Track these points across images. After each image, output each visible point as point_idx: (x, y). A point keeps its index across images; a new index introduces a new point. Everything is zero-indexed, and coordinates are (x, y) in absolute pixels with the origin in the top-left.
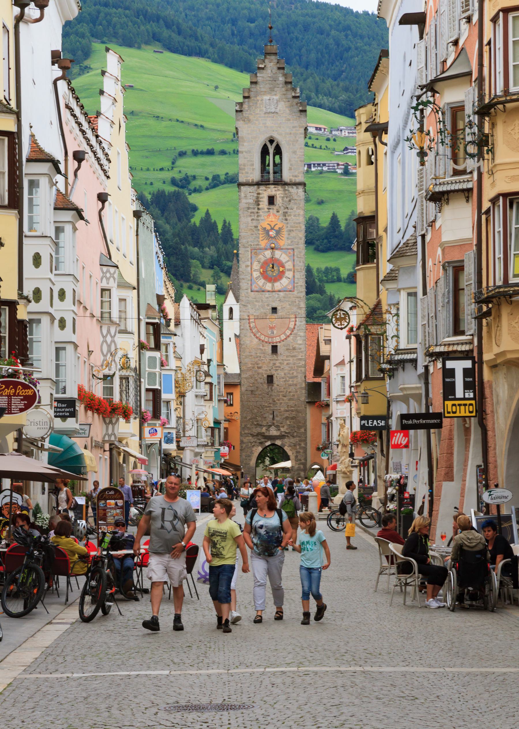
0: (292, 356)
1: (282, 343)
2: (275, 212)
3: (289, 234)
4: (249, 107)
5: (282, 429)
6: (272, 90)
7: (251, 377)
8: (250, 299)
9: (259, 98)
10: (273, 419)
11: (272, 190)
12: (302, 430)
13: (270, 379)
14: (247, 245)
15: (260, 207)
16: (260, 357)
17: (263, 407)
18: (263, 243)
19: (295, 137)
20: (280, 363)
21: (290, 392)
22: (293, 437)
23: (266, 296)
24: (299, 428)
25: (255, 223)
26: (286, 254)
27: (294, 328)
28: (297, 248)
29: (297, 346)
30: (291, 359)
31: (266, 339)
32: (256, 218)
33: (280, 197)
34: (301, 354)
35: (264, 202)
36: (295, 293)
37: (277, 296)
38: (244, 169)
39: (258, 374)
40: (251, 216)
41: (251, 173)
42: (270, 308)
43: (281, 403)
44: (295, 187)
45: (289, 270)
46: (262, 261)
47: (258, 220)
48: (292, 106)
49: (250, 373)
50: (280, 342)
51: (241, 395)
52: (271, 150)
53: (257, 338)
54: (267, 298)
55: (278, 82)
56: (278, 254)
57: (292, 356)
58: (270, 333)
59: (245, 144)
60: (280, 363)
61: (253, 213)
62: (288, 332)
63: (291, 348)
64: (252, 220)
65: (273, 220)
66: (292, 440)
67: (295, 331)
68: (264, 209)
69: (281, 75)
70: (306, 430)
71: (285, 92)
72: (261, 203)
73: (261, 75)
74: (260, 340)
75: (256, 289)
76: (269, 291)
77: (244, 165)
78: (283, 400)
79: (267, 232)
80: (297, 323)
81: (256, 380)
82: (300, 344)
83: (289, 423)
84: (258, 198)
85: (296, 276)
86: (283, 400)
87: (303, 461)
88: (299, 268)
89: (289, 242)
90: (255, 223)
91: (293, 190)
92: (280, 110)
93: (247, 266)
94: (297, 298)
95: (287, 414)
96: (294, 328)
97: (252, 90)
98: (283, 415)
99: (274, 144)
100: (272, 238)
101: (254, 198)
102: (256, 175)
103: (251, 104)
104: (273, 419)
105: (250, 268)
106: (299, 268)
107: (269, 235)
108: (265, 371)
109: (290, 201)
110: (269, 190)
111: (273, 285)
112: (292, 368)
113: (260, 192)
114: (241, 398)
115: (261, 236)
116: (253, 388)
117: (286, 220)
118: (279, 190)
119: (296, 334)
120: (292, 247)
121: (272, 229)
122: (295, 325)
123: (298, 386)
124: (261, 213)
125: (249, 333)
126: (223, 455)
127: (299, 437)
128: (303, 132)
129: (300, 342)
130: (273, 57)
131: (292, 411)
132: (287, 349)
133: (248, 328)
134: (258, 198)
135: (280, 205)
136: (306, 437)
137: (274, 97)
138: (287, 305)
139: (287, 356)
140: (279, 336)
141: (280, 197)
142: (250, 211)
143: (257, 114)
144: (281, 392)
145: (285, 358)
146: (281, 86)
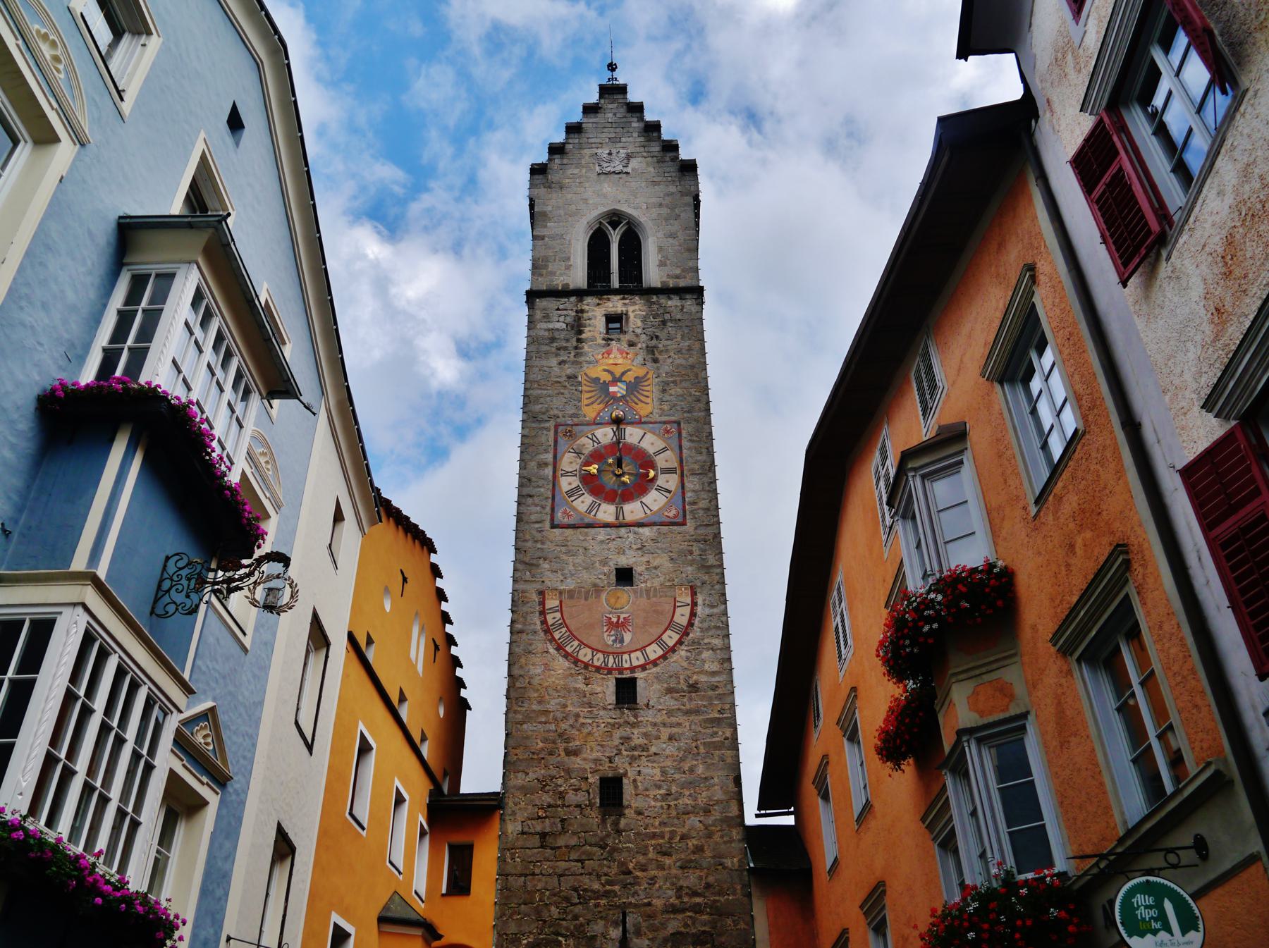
0: (688, 713)
2: (624, 346)
3: (664, 391)
6: (614, 141)
7: (543, 784)
9: (587, 152)
11: (616, 304)
13: (611, 789)
14: (545, 417)
15: (583, 336)
16: (577, 716)
17: (584, 896)
20: (645, 735)
21: (683, 837)
23: (600, 537)
27: (690, 624)
28: (688, 421)
29: (703, 678)
31: (598, 660)
37: (631, 536)
39: (568, 772)
40: (557, 355)
46: (586, 452)
49: (537, 772)
50: (643, 667)
51: (502, 850)
52: (615, 237)
53: (567, 655)
54: (602, 542)
56: (632, 435)
57: (688, 713)
58: (610, 640)
60: (645, 735)
61: (565, 348)
62: (671, 638)
65: (620, 361)
67: (695, 634)
68: (593, 339)
72: (586, 329)
74: (576, 661)
75: (566, 521)
76: (607, 525)
78: (661, 867)
80: (699, 609)
81: (562, 795)
82: (714, 674)
86: (661, 867)
88: (696, 467)
93: (542, 465)
95: (674, 925)
96: (690, 624)
98: (664, 925)
99: (621, 230)
103: (565, 161)
107: (607, 393)
108: (591, 759)
109: (664, 323)
111: (620, 511)
113: (586, 307)
114: (502, 860)
116: (547, 826)
117: (655, 361)
118: (635, 304)
119: (696, 643)
120: (673, 418)
121: (615, 381)
122: (693, 614)
123: (716, 814)
124: (586, 348)
125: (540, 642)
131: (697, 909)
132: (670, 691)
133: (538, 627)
135: (639, 331)
138: (662, 560)
139: (670, 713)
140: (642, 649)
144: (654, 836)
146: (635, 135)
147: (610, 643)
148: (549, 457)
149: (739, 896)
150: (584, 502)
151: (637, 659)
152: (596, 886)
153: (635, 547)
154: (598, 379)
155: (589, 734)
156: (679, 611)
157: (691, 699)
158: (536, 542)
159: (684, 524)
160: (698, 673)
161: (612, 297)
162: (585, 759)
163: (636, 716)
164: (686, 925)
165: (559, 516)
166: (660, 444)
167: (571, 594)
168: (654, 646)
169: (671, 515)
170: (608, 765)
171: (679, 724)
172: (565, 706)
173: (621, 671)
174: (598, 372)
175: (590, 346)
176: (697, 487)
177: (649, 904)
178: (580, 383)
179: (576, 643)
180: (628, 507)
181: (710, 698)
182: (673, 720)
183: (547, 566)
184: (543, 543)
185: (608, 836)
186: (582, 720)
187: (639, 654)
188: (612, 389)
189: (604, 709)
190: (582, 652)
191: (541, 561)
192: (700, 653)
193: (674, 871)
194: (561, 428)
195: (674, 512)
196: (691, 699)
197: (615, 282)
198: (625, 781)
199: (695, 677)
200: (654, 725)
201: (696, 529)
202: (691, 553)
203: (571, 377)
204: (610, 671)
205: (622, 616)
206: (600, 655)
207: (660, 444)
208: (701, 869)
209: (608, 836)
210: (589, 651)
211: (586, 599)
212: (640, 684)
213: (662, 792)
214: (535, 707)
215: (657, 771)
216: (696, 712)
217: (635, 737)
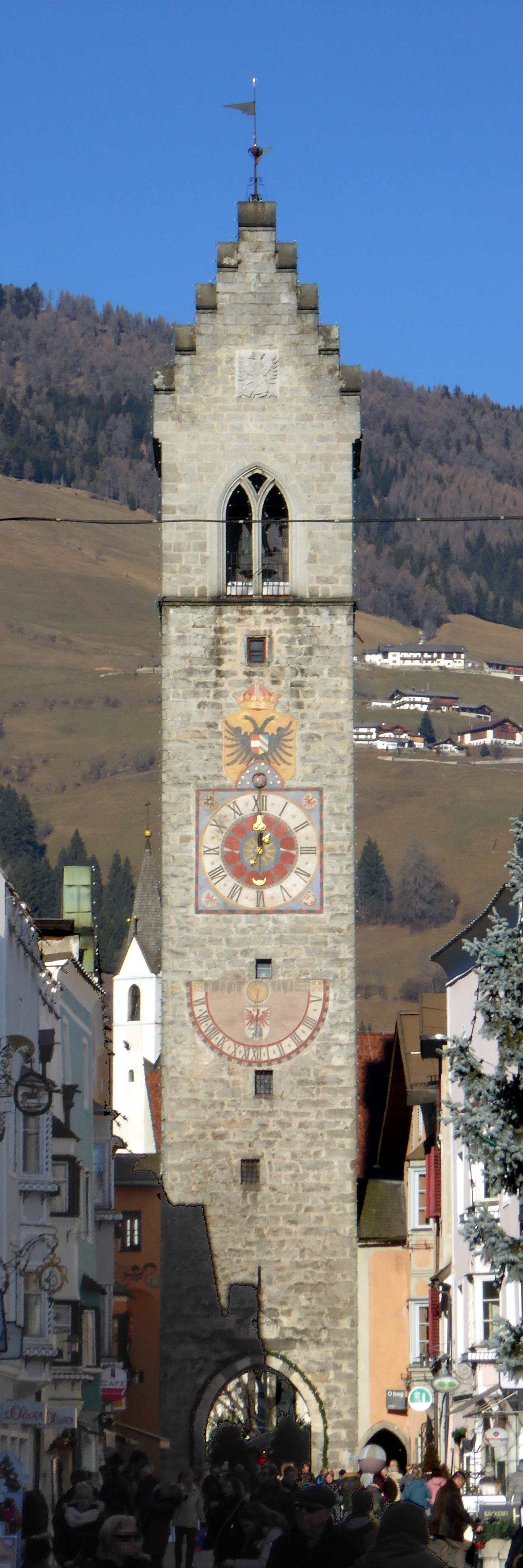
0: (315, 1104)
1: (287, 1063)
2: (268, 684)
3: (308, 748)
4: (193, 379)
5: (285, 1321)
6: (259, 330)
8: (194, 934)
9: (222, 353)
11: (258, 620)
12: (345, 1324)
13: (250, 1169)
15: (223, 668)
18: (231, 775)
19: (327, 469)
20: (281, 1123)
21: (308, 1209)
22: (318, 1343)
24: (336, 1315)
25: (208, 715)
26: (299, 805)
27: (322, 1019)
28: (331, 787)
29: (331, 1073)
30: (313, 1111)
32: (211, 700)
33: (281, 639)
34: (341, 1098)
35: (236, 658)
36: (325, 915)
37: (271, 925)
38: (179, 559)
39: (216, 1155)
40: (196, 694)
41: (199, 571)
42: (251, 960)
43: (282, 1243)
44: (325, 612)
45: (309, 851)
46: (228, 825)
47: (219, 706)
48: (315, 376)
50: (279, 1060)
52: (257, 503)
53: (213, 1047)
54: (243, 931)
55: (278, 309)
57: (315, 1104)
58: (250, 1033)
59: (182, 486)
60: (281, 1123)
61: (204, 684)
62: (304, 1033)
63: (312, 1078)
64: (201, 705)
65: (262, 705)
66: (314, 1353)
68: (234, 674)
69: (285, 289)
70: (354, 1323)
71: (297, 338)
72: (226, 657)
73: (228, 288)
74: (221, 1053)
75: (209, 906)
76: (247, 912)
77: (179, 547)
79: (242, 739)
80: (330, 1004)
82: (340, 1068)
83: (305, 1303)
85: (327, 869)
86: (289, 1233)
87: (347, 1417)
88: (337, 844)
89: (309, 769)
90: (208, 715)
91: (320, 619)
92: (282, 389)
93: (186, 839)
94: (331, 930)
96: (322, 1019)
97: (202, 329)
98: (290, 1276)
99: (266, 489)
101: (207, 642)
103: (199, 371)
105: (193, 843)
106: (337, 844)
107: (249, 749)
109: (310, 651)
110: (250, 620)
111: (260, 896)
112: (314, 1137)
113: (225, 624)
115: (225, 752)
117: (300, 706)
118: (278, 620)
121: (259, 731)
122: (325, 1010)
123: (334, 1192)
124: (226, 687)
126: (111, 1396)
127: (336, 1344)
128: (349, 452)
129: (338, 1061)
130: (263, 236)
131: (315, 1265)
132: (301, 1082)
133: (187, 1018)
134: (217, 641)
135: (283, 662)
136: (355, 1345)
137: (266, 351)
141: (281, 639)
142: (192, 679)
143: (217, 400)
145: (294, 1108)
146: (285, 319)
147: (251, 1036)
148: (191, 831)
149: (348, 1257)
150: (226, 884)
151: (273, 1053)
152: (239, 1246)
153: (274, 936)
154: (238, 729)
155: (233, 1121)
156: (312, 1006)
157: (318, 1091)
158: (182, 928)
159: (320, 911)
160: (327, 1067)
161: (253, 608)
162: (229, 1143)
163: (272, 1106)
164: (306, 1277)
165: (203, 899)
166: (301, 818)
167: (216, 986)
168: (289, 1041)
169: (309, 902)
170: (248, 1148)
171: (308, 1114)
172: (212, 1095)
173: (260, 1063)
175: (231, 684)
176: (337, 871)
177: (279, 1261)
178: (220, 733)
179: (220, 1036)
180: (268, 892)
181: (335, 1091)
182: (303, 1110)
183: (192, 955)
184: (188, 930)
185: (248, 1207)
186: (226, 1108)
187: (275, 1047)
188: (254, 744)
189: (245, 1098)
190: (226, 1045)
191: (187, 949)
192: (329, 1047)
193: (299, 1237)
194: (203, 794)
195: (312, 899)
196: (318, 1091)
197: (256, 567)
198: (261, 1162)
199: (323, 1071)
200: (287, 1114)
201: (332, 917)
202: (326, 943)
203: (212, 725)
204: (250, 1063)
205: (262, 1010)
206: (241, 1048)
207: (301, 818)
208: (320, 1234)
209: (248, 1207)
210: (232, 1044)
211: (229, 992)
212: (275, 1075)
213: (292, 1172)
214: (187, 1095)
215: (288, 1155)
216: (324, 1102)
217: (271, 1124)
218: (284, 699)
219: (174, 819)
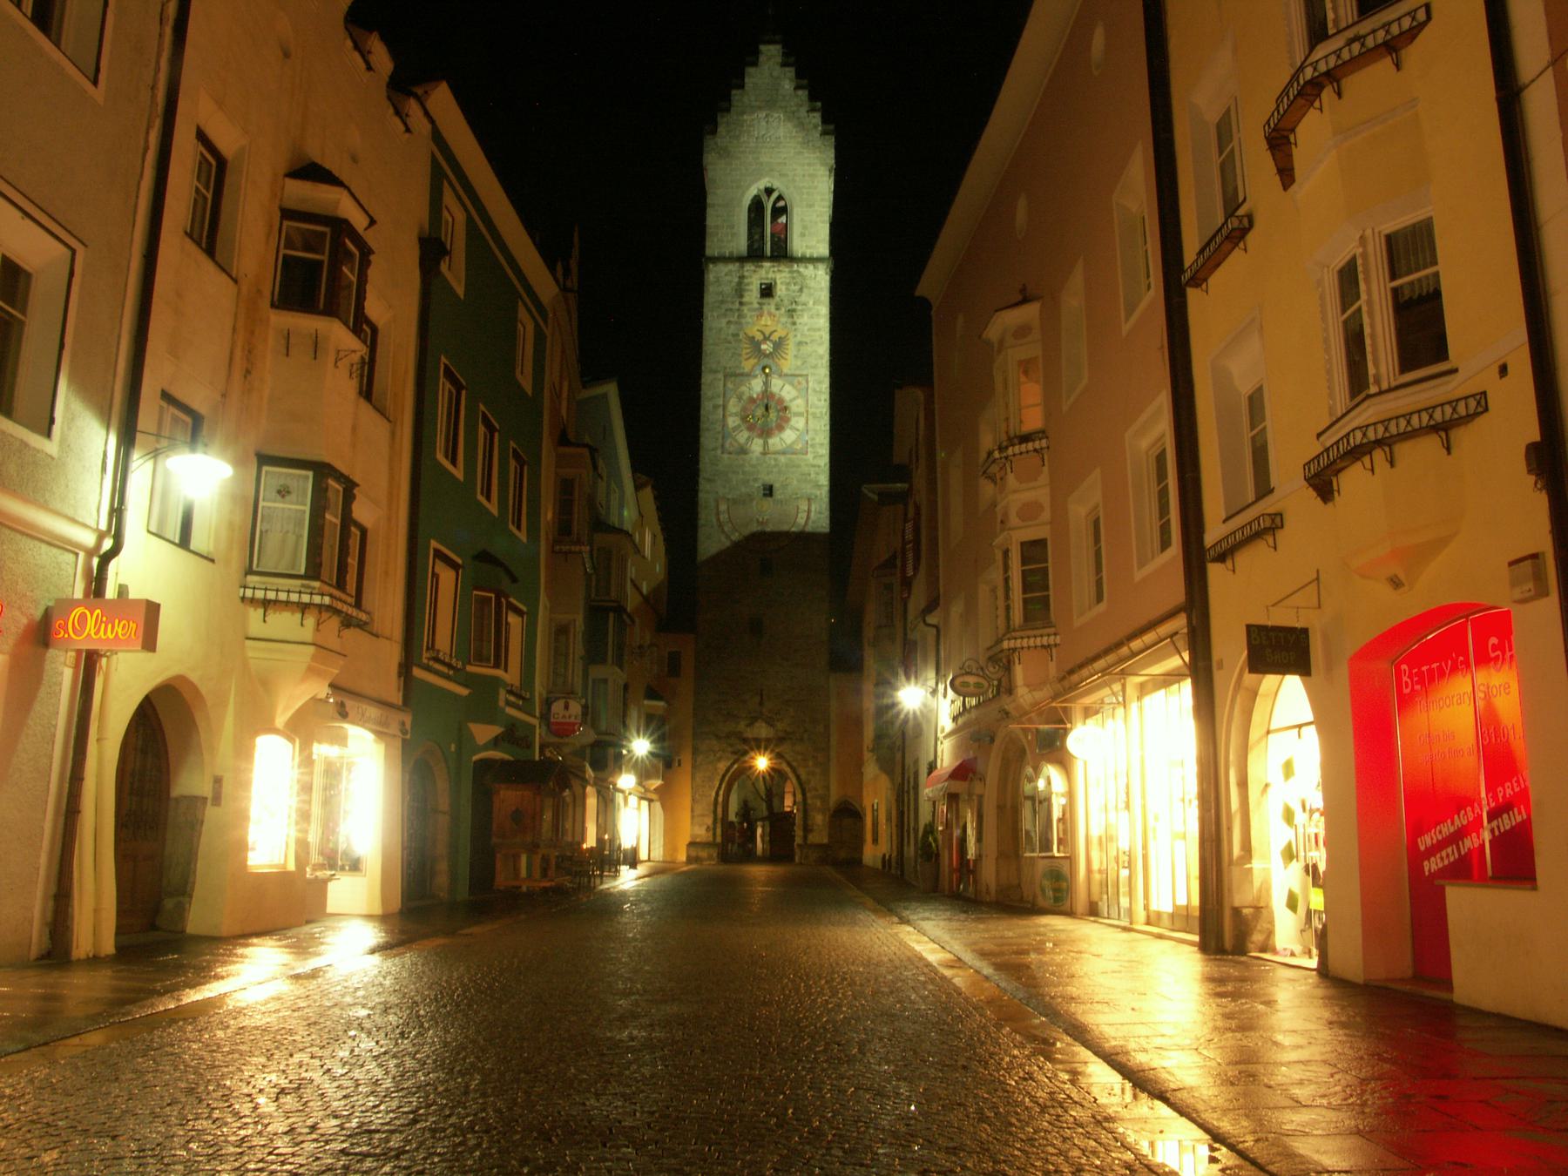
2: (772, 308)
10: (761, 704)
35: (753, 295)
36: (810, 456)
44: (811, 267)
56: (776, 384)
64: (729, 322)
70: (827, 727)
84: (740, 283)
93: (716, 407)
100: (767, 356)
102: (741, 244)
104: (761, 704)
109: (801, 290)
110: (762, 273)
111: (766, 444)
121: (766, 339)
124: (745, 309)
134: (740, 283)
150: (743, 436)
174: (754, 331)
180: (771, 441)
207: (794, 393)
218: (784, 320)
219: (709, 394)
